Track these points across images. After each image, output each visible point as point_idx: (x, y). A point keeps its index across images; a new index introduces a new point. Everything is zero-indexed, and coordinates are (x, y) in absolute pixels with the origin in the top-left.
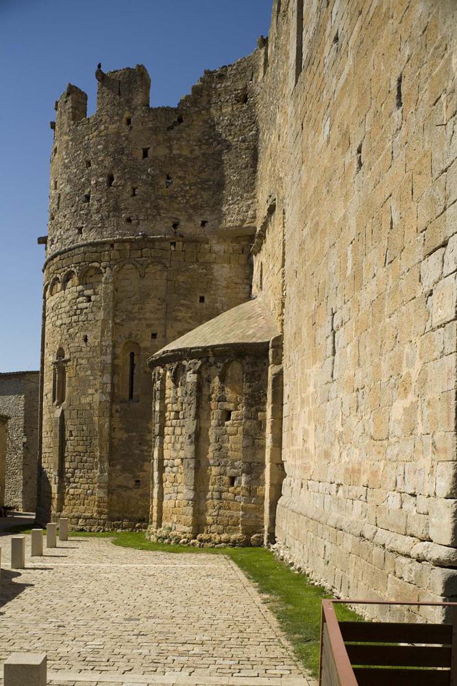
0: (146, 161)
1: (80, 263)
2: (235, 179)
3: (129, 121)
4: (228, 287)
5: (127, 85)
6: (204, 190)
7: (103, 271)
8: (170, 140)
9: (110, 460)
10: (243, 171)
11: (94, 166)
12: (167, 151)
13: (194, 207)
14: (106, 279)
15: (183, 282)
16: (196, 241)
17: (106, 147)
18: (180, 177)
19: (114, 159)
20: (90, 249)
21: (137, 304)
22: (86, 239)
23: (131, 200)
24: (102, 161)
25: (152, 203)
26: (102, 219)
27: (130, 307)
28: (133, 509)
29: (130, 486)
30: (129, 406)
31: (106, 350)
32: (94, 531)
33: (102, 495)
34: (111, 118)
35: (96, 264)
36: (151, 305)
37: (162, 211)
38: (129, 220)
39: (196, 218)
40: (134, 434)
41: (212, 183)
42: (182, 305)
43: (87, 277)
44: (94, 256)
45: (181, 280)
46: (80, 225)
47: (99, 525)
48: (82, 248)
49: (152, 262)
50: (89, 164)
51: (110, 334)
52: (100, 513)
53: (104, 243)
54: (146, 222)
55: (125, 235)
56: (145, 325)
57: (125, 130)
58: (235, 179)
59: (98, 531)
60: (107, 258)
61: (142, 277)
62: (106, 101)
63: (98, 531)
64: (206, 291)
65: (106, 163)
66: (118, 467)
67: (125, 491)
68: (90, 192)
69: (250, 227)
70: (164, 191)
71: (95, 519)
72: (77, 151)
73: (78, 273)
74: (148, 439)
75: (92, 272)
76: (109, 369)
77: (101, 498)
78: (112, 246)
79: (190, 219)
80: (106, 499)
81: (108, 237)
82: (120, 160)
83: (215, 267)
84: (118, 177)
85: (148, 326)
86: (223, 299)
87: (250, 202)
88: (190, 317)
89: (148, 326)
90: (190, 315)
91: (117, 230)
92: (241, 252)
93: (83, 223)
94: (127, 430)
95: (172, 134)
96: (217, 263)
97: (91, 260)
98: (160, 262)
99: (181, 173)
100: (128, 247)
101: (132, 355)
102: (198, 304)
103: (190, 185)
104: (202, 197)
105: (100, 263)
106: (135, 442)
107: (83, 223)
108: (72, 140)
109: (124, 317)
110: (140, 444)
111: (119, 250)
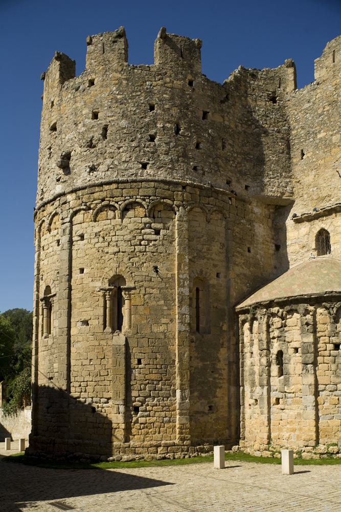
0: (206, 122)
1: (150, 196)
2: (274, 159)
3: (191, 83)
4: (263, 243)
6: (247, 161)
7: (176, 209)
8: (222, 111)
9: (191, 387)
10: (280, 155)
11: (159, 111)
12: (222, 120)
13: (240, 172)
14: (180, 217)
15: (237, 232)
16: (243, 201)
17: (172, 98)
18: (230, 145)
19: (181, 112)
20: (162, 185)
21: (206, 245)
22: (154, 176)
24: (168, 109)
25: (213, 159)
26: (172, 160)
27: (199, 247)
28: (209, 433)
29: (207, 411)
30: (203, 337)
31: (184, 283)
32: (179, 458)
33: (184, 421)
34: (176, 75)
35: (169, 202)
36: (216, 247)
37: (221, 169)
38: (195, 168)
39: (241, 181)
40: (208, 363)
41: (252, 157)
42: (238, 252)
43: (158, 212)
44: (167, 193)
45: (237, 231)
46: (145, 160)
47: (182, 451)
48: (153, 183)
49: (215, 211)
50: (152, 108)
51: (186, 268)
52: (183, 439)
53: (177, 184)
54: (210, 175)
55: (194, 181)
56: (212, 265)
58: (274, 159)
59: (184, 457)
60: (180, 198)
61: (208, 221)
62: (169, 57)
63: (184, 457)
64: (251, 243)
66: (196, 394)
67: (202, 416)
68: (156, 133)
69: (289, 199)
70: (220, 152)
71: (178, 445)
72: (136, 92)
73: (148, 206)
74: (218, 367)
75: (161, 207)
76: (188, 301)
77: (183, 424)
78: (184, 188)
79: (238, 181)
80: (188, 425)
81: (179, 179)
82: (186, 115)
83: (256, 225)
84: (185, 128)
85: (215, 266)
86: (260, 252)
87: (288, 180)
88: (244, 263)
89: (215, 266)
90: (243, 261)
91: (187, 174)
92: (268, 217)
93: (149, 160)
94: (202, 359)
95: (224, 106)
96: (256, 222)
97: (163, 196)
98: (221, 212)
99: (231, 142)
100: (198, 193)
101: (198, 290)
102: (248, 254)
103: (237, 153)
104: (245, 166)
105: (173, 201)
106: (209, 370)
107: (149, 160)
109: (195, 255)
110: (212, 372)
111: (191, 193)
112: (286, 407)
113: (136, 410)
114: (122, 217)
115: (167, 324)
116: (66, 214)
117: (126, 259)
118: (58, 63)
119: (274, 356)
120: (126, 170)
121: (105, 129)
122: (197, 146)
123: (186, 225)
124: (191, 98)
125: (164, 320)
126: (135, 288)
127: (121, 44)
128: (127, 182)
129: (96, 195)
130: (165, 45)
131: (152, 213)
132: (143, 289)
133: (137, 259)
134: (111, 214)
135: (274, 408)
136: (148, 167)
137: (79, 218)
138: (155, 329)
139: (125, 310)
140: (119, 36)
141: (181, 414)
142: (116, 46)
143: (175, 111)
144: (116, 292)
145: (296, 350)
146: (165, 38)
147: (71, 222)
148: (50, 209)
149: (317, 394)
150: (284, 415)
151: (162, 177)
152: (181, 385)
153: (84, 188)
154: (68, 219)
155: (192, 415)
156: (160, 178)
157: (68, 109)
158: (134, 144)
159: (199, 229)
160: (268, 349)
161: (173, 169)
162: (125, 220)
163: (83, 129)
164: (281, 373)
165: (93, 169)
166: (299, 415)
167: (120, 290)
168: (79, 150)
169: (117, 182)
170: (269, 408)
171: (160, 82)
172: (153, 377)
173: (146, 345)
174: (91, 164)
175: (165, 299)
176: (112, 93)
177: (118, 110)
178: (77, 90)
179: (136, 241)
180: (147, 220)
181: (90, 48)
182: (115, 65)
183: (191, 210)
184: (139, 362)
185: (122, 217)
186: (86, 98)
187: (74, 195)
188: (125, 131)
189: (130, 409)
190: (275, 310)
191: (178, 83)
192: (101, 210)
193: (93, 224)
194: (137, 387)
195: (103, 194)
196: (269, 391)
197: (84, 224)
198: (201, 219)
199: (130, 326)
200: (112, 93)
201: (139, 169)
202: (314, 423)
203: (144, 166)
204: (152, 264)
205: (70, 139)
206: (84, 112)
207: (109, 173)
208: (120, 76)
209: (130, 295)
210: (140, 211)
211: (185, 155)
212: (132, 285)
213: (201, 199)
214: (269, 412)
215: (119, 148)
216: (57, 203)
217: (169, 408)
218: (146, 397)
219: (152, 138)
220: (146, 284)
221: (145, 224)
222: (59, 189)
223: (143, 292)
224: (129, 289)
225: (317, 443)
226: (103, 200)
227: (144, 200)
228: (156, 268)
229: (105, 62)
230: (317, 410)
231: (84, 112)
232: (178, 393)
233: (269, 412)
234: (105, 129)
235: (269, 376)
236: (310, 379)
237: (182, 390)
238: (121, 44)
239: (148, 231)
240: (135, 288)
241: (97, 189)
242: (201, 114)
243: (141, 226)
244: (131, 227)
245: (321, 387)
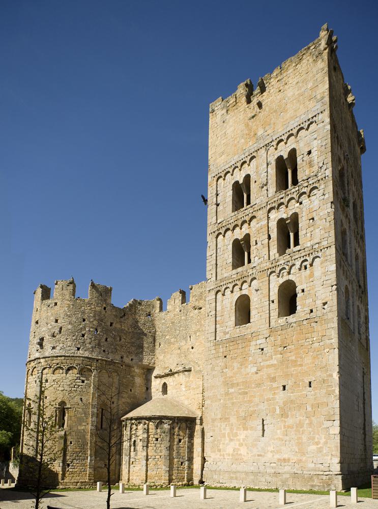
3: (105, 308)
5: (104, 293)
7: (93, 371)
9: (95, 455)
11: (87, 322)
17: (94, 316)
23: (105, 343)
26: (92, 347)
33: (91, 471)
35: (89, 367)
38: (104, 351)
43: (84, 372)
44: (89, 363)
46: (79, 346)
50: (84, 320)
53: (94, 359)
57: (103, 312)
62: (95, 295)
65: (94, 323)
75: (86, 370)
76: (96, 415)
82: (101, 324)
100: (105, 363)
108: (73, 305)
112: (136, 465)
113: (68, 465)
114: (66, 373)
115: (85, 426)
116: (40, 369)
117: (67, 394)
118: (41, 289)
119: (133, 442)
120: (69, 350)
121: (61, 328)
122: (106, 340)
123: (97, 379)
124: (104, 316)
125: (84, 424)
126: (71, 408)
127: (71, 287)
128: (69, 356)
129: (54, 361)
130: (93, 289)
131: (81, 372)
132: (74, 409)
133: (72, 394)
134: (61, 371)
135: (131, 466)
136: (80, 349)
137: (45, 372)
138: (79, 428)
139: (66, 418)
140: (71, 283)
141: (89, 468)
142: (69, 288)
143: (95, 322)
144: (62, 410)
145: (141, 440)
146: (93, 285)
147: (42, 373)
148: (33, 364)
149: (147, 460)
150: (135, 469)
151: (87, 356)
152: (90, 454)
153: (49, 357)
154: (40, 371)
155: (95, 468)
156: (86, 356)
157: (44, 315)
158: (74, 338)
159: (104, 381)
160: (130, 439)
161: (92, 351)
162: (68, 375)
163: (50, 327)
164: (135, 451)
165: (54, 348)
166: (140, 469)
167: (64, 409)
168: (48, 337)
169: (65, 356)
170: (129, 466)
171: (89, 308)
172: (77, 450)
173: (74, 435)
174: (53, 345)
175: (85, 414)
176: (65, 311)
177: (67, 320)
178: (48, 306)
179: (72, 386)
180: (78, 375)
181: (56, 286)
182: (67, 297)
183: (100, 371)
184: (71, 443)
185: (66, 373)
186: (53, 311)
187: (44, 359)
188: (70, 331)
189: (65, 465)
190: (133, 421)
191: (98, 309)
192: (56, 369)
193: (52, 375)
194: (69, 454)
195: (58, 361)
196: (130, 458)
197: (48, 375)
198: (106, 376)
199: (67, 426)
200: (65, 311)
201: (76, 350)
202: (145, 473)
203: (78, 349)
204: (80, 397)
205: (44, 331)
206: (51, 318)
207: (61, 351)
208: (69, 303)
209: (68, 411)
210: (75, 371)
211: (99, 345)
212: (69, 406)
213: (105, 366)
214: (129, 468)
215: (67, 339)
216: (36, 362)
217: (84, 465)
218: (73, 460)
219: (83, 336)
220: (76, 406)
221: (77, 377)
222: (37, 355)
223: (74, 410)
224: (68, 408)
225: (146, 481)
226: (58, 364)
227: (77, 366)
228: (81, 399)
229: (63, 295)
230: (147, 467)
231: (51, 318)
232: (89, 457)
233: (129, 468)
234: (61, 328)
235: (130, 451)
236: (145, 454)
237: (91, 457)
238: (71, 287)
239: (78, 381)
240: (71, 408)
241: (55, 358)
242: (109, 324)
243: (75, 378)
244: (70, 378)
245: (149, 457)
